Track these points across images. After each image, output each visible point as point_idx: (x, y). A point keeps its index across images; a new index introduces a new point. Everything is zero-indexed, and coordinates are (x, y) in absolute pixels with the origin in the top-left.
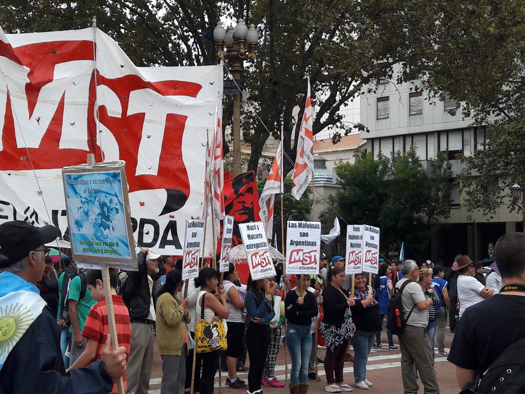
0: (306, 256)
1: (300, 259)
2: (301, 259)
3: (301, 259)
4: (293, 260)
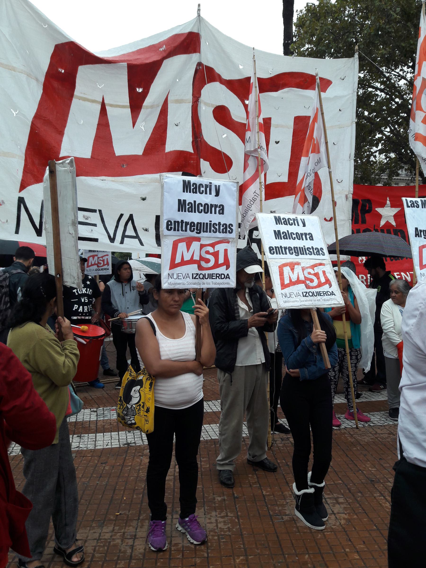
0: (207, 252)
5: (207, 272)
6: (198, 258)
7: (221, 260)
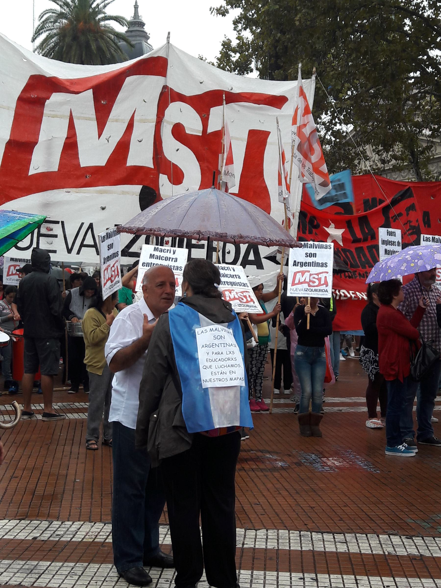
0: (314, 278)
1: (306, 281)
3: (307, 280)
5: (313, 288)
7: (322, 282)
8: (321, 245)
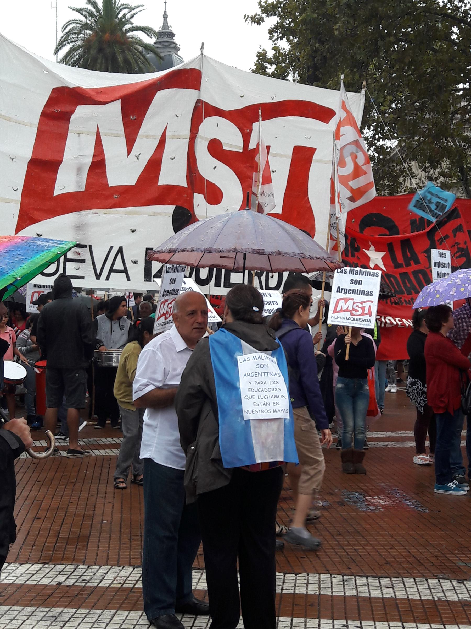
0: (357, 306)
1: (349, 309)
2: (350, 308)
3: (350, 308)
4: (339, 309)
5: (356, 317)
6: (351, 309)
7: (366, 311)
8: (368, 272)
